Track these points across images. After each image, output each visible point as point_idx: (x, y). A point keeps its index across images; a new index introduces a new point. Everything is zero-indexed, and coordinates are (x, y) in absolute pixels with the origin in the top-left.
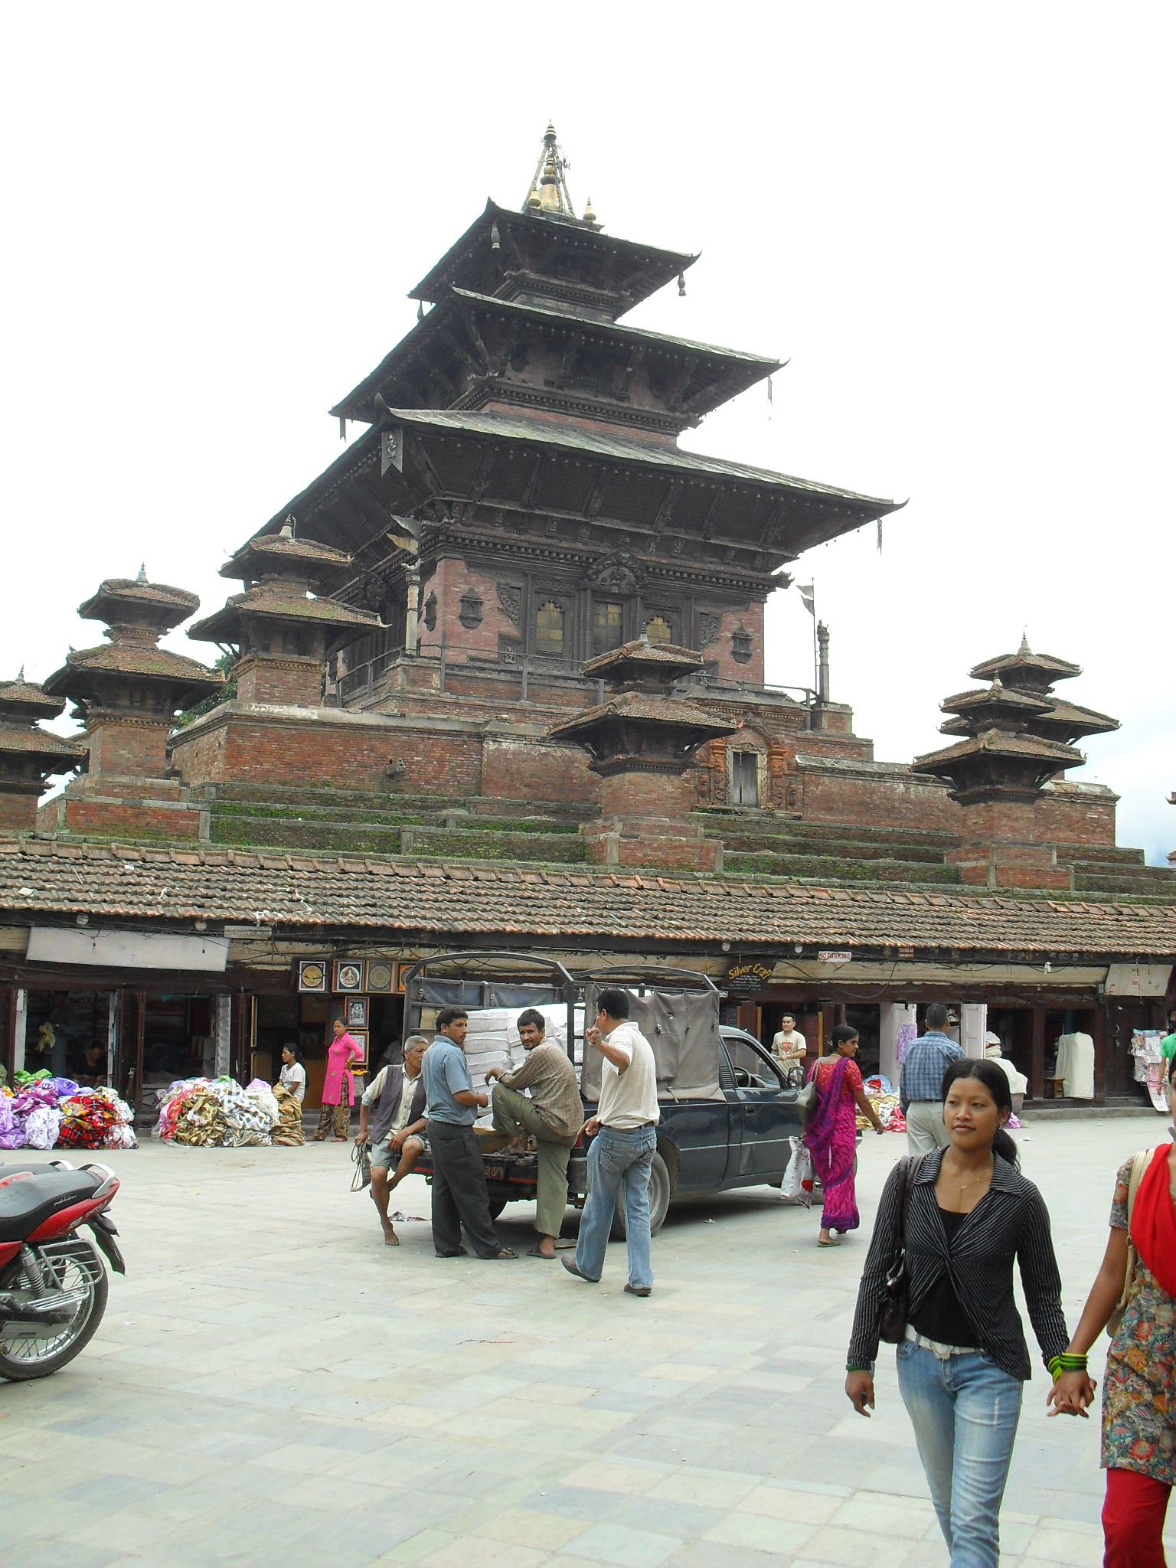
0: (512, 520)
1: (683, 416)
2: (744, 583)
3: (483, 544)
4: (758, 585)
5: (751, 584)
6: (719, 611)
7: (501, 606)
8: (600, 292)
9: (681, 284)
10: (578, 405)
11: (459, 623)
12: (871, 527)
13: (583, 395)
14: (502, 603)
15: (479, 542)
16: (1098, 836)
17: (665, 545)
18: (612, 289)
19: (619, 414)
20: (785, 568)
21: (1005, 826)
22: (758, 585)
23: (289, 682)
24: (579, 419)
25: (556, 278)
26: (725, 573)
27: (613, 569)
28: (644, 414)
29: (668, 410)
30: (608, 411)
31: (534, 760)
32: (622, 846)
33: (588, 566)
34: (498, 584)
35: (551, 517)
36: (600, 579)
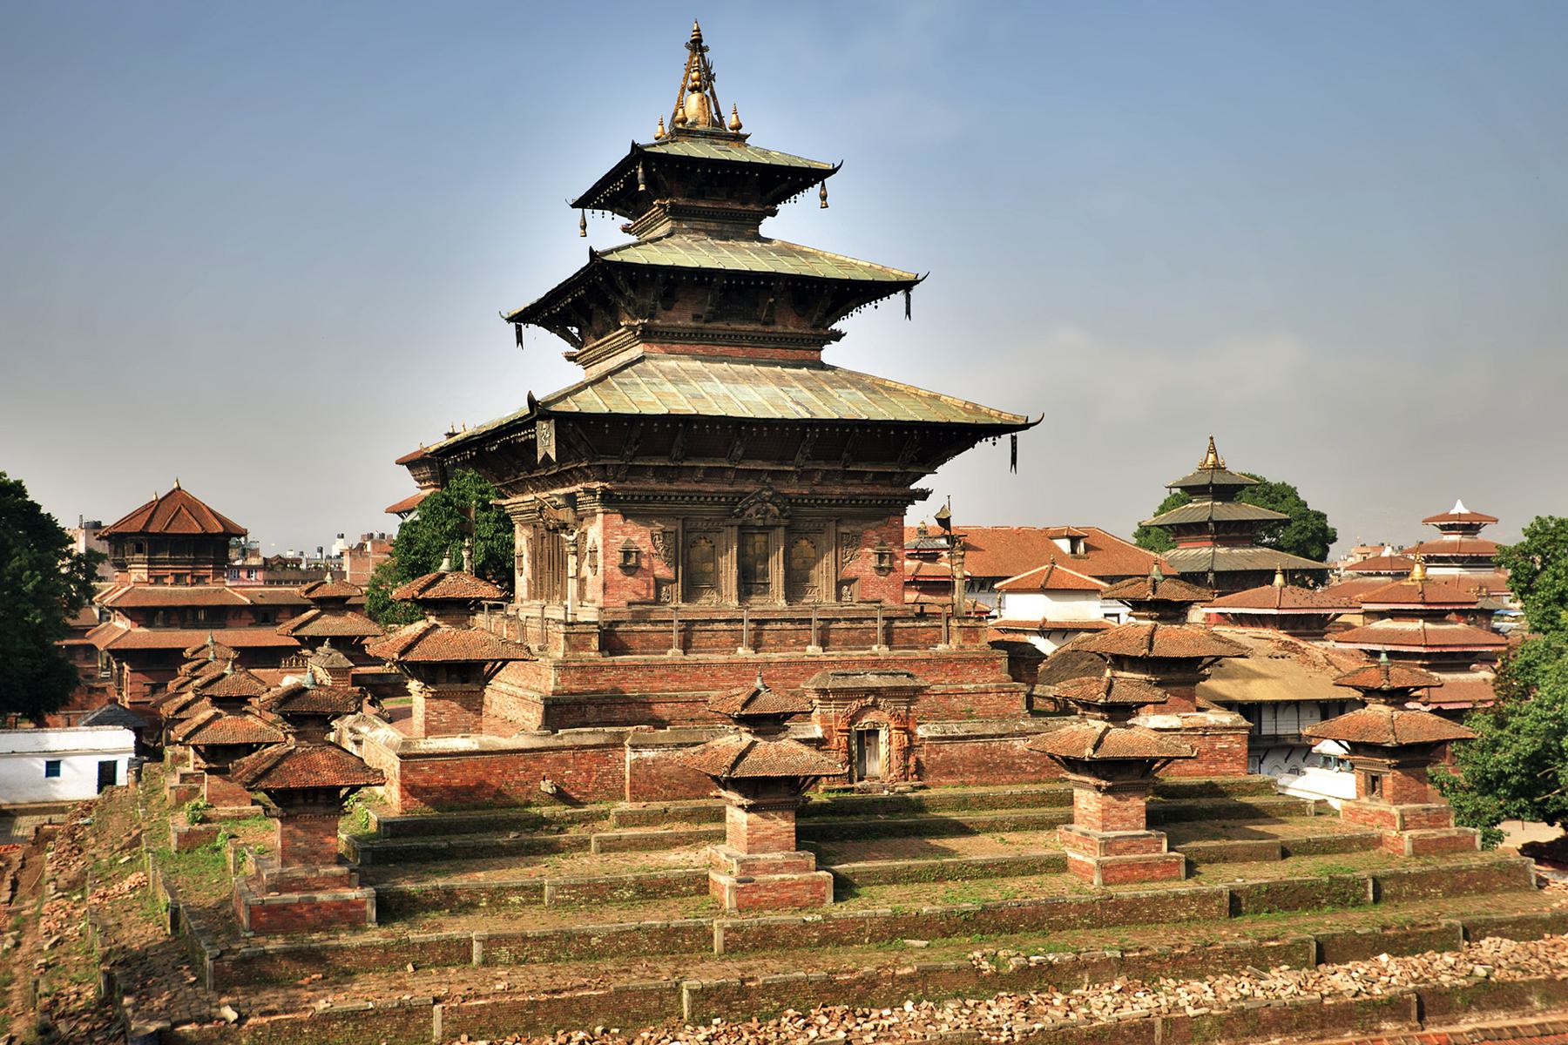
0: (659, 472)
2: (883, 501)
4: (896, 501)
6: (859, 529)
10: (724, 336)
11: (618, 571)
15: (633, 496)
16: (1228, 765)
17: (804, 476)
21: (1114, 816)
24: (726, 348)
26: (864, 495)
27: (758, 506)
30: (753, 337)
31: (671, 763)
32: (739, 891)
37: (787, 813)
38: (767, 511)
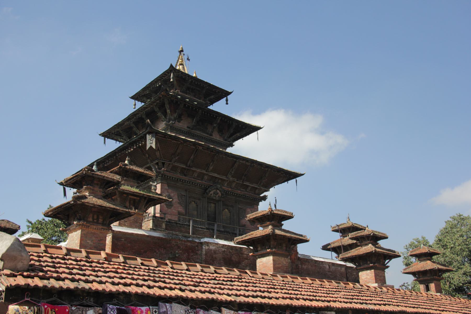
1: (229, 143)
2: (253, 198)
3: (174, 179)
4: (257, 199)
5: (255, 199)
7: (179, 201)
8: (199, 100)
9: (227, 100)
10: (197, 136)
12: (292, 182)
13: (198, 132)
14: (179, 200)
18: (203, 100)
19: (210, 140)
20: (265, 194)
21: (378, 279)
22: (257, 199)
23: (131, 220)
25: (186, 94)
26: (248, 194)
27: (215, 190)
28: (217, 141)
29: (224, 140)
30: (206, 139)
33: (206, 189)
34: (178, 193)
35: (196, 171)
36: (210, 194)
37: (285, 258)
38: (218, 193)
